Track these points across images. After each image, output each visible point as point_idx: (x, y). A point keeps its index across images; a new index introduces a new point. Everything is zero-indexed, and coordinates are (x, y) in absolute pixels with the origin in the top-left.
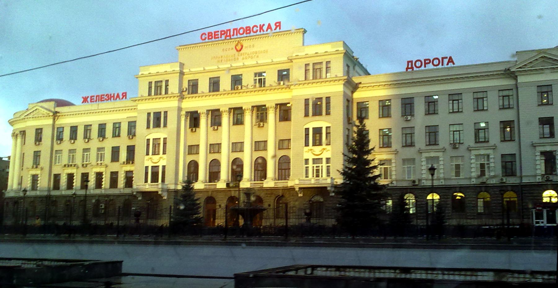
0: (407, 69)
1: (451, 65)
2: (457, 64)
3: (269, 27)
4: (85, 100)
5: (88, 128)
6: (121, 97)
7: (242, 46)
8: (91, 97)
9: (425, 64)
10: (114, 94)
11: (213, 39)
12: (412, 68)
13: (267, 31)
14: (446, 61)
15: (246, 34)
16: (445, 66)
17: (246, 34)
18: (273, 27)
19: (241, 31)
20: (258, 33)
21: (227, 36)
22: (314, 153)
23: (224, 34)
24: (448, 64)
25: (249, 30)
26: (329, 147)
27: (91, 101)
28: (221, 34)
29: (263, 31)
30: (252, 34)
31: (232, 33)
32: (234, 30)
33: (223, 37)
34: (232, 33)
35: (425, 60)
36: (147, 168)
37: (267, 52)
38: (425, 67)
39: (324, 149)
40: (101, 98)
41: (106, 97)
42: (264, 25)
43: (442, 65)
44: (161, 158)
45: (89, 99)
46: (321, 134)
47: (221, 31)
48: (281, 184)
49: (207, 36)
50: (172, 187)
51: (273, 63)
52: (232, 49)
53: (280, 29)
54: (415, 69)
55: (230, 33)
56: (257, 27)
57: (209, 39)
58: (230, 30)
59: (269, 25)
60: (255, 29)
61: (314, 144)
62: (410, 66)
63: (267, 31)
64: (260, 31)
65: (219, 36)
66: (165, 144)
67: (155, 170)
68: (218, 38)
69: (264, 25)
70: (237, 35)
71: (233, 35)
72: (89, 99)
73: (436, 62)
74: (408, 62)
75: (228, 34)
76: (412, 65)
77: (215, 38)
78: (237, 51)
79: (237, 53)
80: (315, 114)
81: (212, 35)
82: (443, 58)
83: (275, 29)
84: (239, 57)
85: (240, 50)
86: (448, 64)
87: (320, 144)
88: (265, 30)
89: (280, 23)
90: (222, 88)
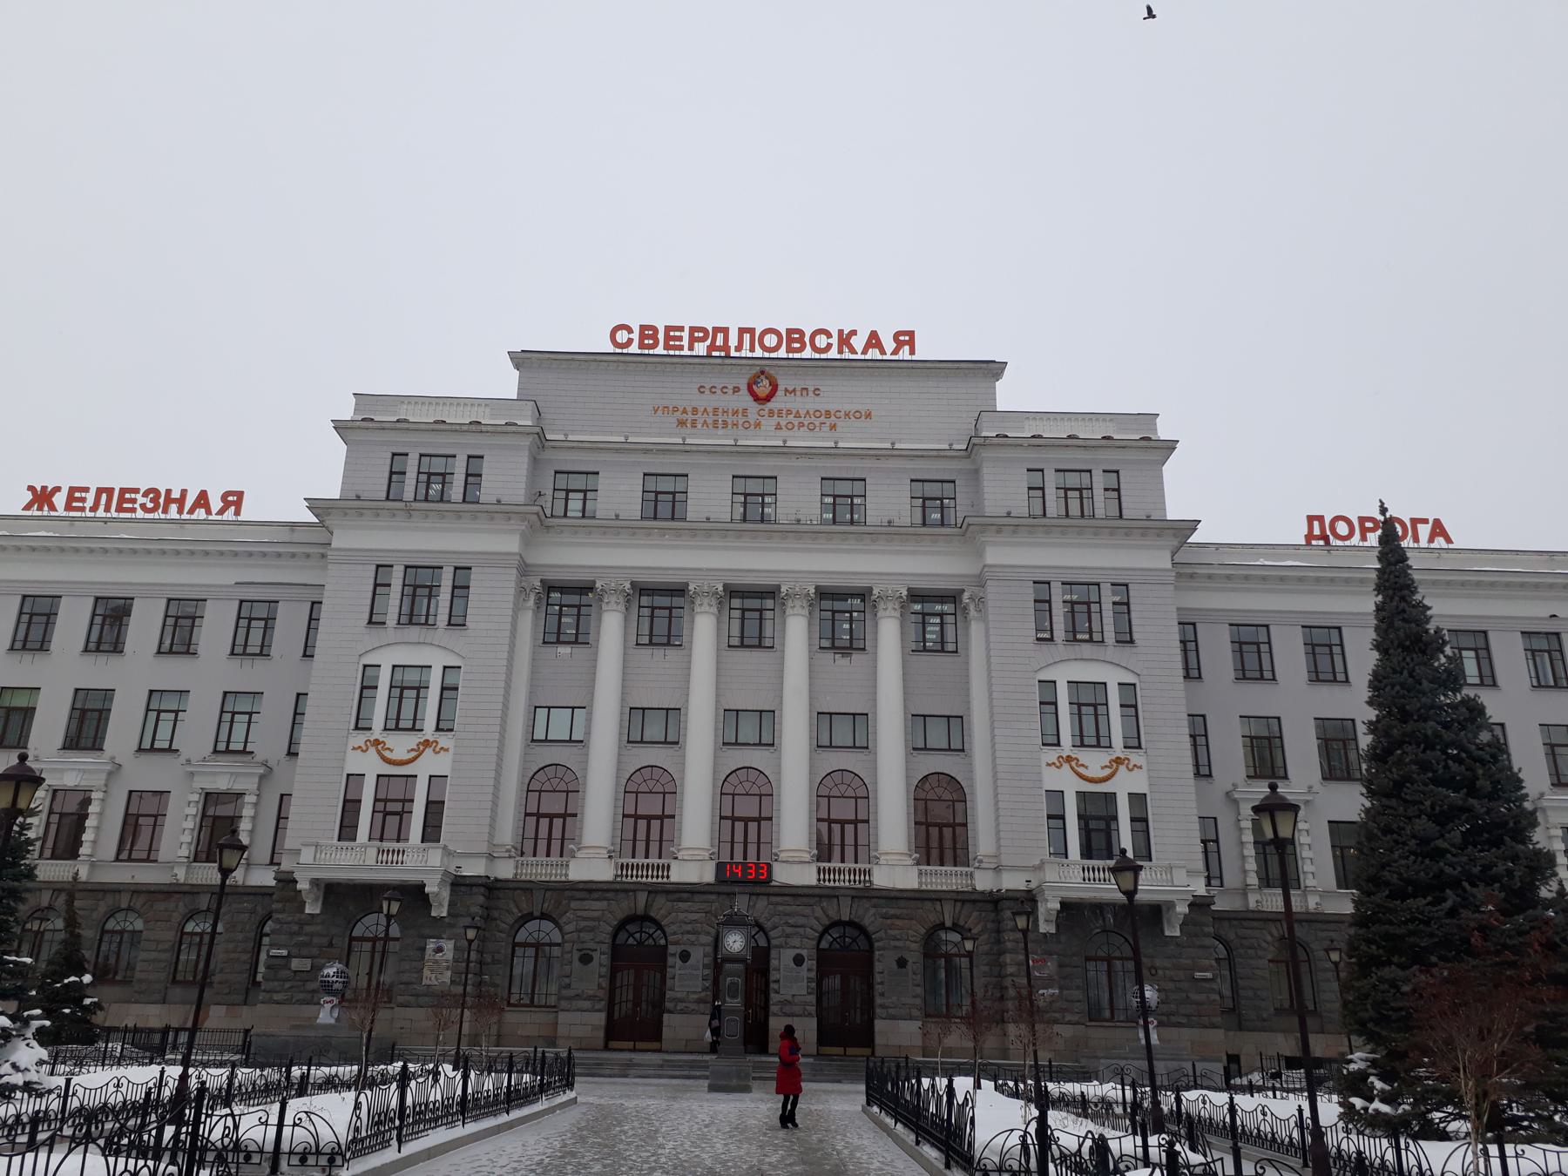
0: (1309, 537)
1: (1440, 542)
3: (874, 340)
7: (775, 388)
8: (72, 490)
10: (184, 492)
12: (1326, 539)
13: (865, 352)
16: (1423, 543)
18: (889, 345)
21: (712, 347)
22: (1081, 770)
24: (1431, 540)
25: (801, 340)
28: (693, 340)
29: (853, 351)
31: (733, 342)
32: (742, 331)
34: (733, 342)
35: (1362, 520)
36: (354, 779)
37: (868, 415)
39: (1118, 761)
40: (122, 500)
41: (141, 499)
42: (854, 333)
47: (693, 330)
48: (946, 879)
49: (635, 336)
50: (474, 868)
51: (892, 454)
52: (736, 390)
53: (912, 352)
54: (1334, 541)
55: (726, 339)
57: (642, 346)
58: (725, 331)
59: (874, 335)
60: (821, 341)
62: (1317, 532)
63: (865, 352)
64: (840, 351)
65: (685, 342)
66: (448, 689)
68: (681, 348)
69: (854, 333)
70: (752, 349)
71: (739, 348)
72: (60, 500)
74: (1311, 519)
75: (720, 341)
77: (667, 347)
78: (757, 398)
79: (753, 407)
80: (1073, 637)
81: (655, 337)
82: (1415, 522)
83: (895, 352)
85: (768, 398)
86: (1431, 540)
87: (1100, 742)
88: (859, 348)
89: (911, 334)
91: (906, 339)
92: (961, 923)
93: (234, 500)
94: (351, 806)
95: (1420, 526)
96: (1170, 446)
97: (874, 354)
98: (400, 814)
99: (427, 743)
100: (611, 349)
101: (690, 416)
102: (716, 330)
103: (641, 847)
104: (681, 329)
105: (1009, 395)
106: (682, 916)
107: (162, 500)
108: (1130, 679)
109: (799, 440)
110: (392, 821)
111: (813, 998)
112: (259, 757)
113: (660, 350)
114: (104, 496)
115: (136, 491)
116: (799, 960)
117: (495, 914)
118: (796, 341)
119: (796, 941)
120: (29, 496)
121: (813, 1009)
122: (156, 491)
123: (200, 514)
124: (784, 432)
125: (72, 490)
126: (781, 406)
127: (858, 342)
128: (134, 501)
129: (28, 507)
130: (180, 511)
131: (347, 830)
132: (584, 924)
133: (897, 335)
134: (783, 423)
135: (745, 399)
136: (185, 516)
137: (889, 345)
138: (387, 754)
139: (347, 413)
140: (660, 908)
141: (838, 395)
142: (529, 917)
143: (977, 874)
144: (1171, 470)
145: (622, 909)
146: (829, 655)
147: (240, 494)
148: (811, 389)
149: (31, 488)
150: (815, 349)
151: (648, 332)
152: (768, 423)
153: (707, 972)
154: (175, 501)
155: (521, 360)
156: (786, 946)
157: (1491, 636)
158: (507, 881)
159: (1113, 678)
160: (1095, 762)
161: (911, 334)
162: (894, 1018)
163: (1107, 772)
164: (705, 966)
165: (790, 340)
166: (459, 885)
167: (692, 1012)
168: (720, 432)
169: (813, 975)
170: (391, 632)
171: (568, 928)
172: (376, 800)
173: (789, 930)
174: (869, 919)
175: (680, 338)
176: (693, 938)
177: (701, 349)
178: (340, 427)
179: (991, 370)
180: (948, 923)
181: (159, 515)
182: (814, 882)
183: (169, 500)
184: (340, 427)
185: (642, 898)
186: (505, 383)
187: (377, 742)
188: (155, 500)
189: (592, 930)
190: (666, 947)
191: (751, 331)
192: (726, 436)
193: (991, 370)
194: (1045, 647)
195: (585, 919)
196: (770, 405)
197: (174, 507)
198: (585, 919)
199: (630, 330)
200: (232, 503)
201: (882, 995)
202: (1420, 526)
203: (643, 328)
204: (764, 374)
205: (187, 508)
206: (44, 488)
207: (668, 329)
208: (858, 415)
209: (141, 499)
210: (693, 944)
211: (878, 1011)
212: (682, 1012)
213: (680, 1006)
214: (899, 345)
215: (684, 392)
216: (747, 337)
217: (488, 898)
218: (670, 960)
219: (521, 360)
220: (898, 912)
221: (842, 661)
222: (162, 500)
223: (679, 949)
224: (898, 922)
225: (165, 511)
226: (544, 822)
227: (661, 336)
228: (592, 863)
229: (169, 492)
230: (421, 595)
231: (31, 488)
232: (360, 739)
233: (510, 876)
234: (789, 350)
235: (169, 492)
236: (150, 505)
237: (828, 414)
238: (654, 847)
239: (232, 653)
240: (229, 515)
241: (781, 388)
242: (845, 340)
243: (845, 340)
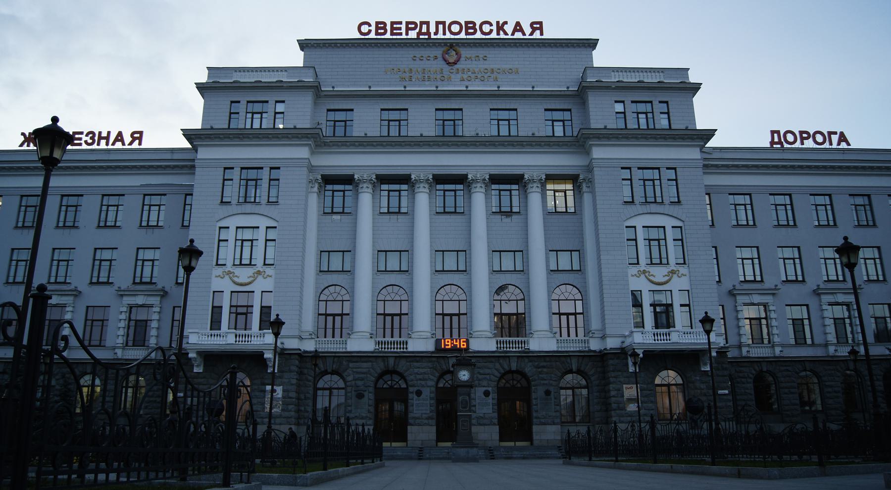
0: (772, 143)
1: (844, 145)
2: (856, 143)
3: (518, 27)
9: (802, 139)
10: (109, 133)
12: (780, 143)
13: (513, 34)
14: (835, 138)
22: (651, 278)
24: (839, 144)
25: (474, 28)
26: (683, 270)
28: (408, 29)
29: (506, 34)
31: (433, 29)
32: (438, 23)
34: (433, 29)
35: (801, 133)
38: (802, 144)
41: (84, 138)
42: (506, 23)
47: (408, 23)
49: (373, 28)
52: (436, 58)
53: (542, 34)
56: (491, 25)
57: (377, 34)
58: (427, 23)
59: (518, 24)
60: (486, 28)
62: (776, 140)
63: (513, 34)
64: (498, 34)
65: (403, 31)
68: (401, 34)
69: (506, 23)
70: (444, 34)
71: (436, 33)
74: (773, 132)
75: (424, 30)
77: (392, 34)
78: (448, 63)
79: (447, 68)
81: (384, 28)
82: (830, 133)
83: (531, 34)
84: (453, 76)
85: (455, 63)
86: (839, 144)
88: (509, 31)
89: (541, 23)
91: (537, 26)
92: (582, 369)
93: (138, 136)
94: (216, 311)
96: (696, 88)
97: (518, 35)
98: (246, 314)
99: (259, 273)
100: (359, 36)
101: (408, 75)
102: (422, 23)
103: (388, 332)
104: (400, 23)
105: (601, 58)
106: (416, 370)
107: (96, 138)
108: (679, 224)
109: (475, 87)
110: (241, 318)
111: (496, 415)
112: (160, 286)
113: (388, 36)
115: (82, 133)
116: (487, 394)
117: (305, 371)
119: (485, 383)
120: (22, 138)
121: (496, 421)
122: (93, 133)
123: (119, 145)
124: (467, 83)
126: (463, 66)
127: (509, 28)
128: (80, 139)
129: (21, 145)
130: (107, 144)
131: (215, 323)
132: (357, 376)
133: (532, 24)
134: (465, 76)
135: (441, 63)
136: (110, 147)
137: (528, 30)
138: (236, 279)
139: (204, 78)
140: (402, 366)
141: (497, 59)
142: (326, 373)
143: (591, 340)
144: (698, 100)
145: (380, 366)
146: (498, 217)
147: (141, 133)
148: (481, 56)
150: (483, 33)
151: (380, 26)
152: (456, 78)
153: (432, 402)
154: (104, 138)
155: (304, 45)
156: (480, 386)
157: (873, 197)
158: (310, 352)
160: (659, 273)
161: (541, 23)
162: (544, 424)
163: (667, 278)
164: (431, 399)
165: (467, 28)
166: (283, 354)
167: (425, 424)
168: (427, 83)
169: (495, 402)
170: (234, 209)
171: (350, 378)
172: (231, 306)
173: (480, 377)
174: (528, 369)
175: (400, 29)
176: (423, 383)
177: (413, 34)
178: (201, 87)
179: (592, 44)
180: (574, 368)
181: (95, 146)
182: (494, 349)
184: (201, 87)
185: (391, 361)
186: (297, 59)
187: (229, 273)
188: (93, 138)
189: (362, 379)
190: (407, 388)
191: (444, 23)
192: (431, 86)
193: (592, 44)
194: (629, 207)
195: (357, 373)
196: (456, 66)
197: (103, 142)
198: (357, 373)
199: (370, 25)
201: (537, 411)
203: (377, 23)
204: (452, 47)
205: (111, 141)
207: (392, 23)
209: (84, 138)
210: (423, 386)
211: (535, 420)
212: (419, 425)
213: (418, 421)
214: (534, 30)
215: (404, 59)
216: (441, 27)
217: (300, 362)
218: (410, 396)
219: (304, 45)
220: (545, 364)
221: (506, 220)
222: (96, 138)
223: (416, 389)
224: (545, 370)
225: (98, 144)
226: (330, 319)
227: (388, 28)
228: (361, 341)
229: (100, 133)
230: (252, 184)
231: (23, 134)
232: (219, 271)
233: (312, 349)
234: (467, 33)
235: (100, 133)
236: (90, 141)
237: (492, 71)
238: (396, 332)
239: (141, 226)
240: (136, 145)
241: (463, 56)
242: (500, 27)
243: (500, 27)
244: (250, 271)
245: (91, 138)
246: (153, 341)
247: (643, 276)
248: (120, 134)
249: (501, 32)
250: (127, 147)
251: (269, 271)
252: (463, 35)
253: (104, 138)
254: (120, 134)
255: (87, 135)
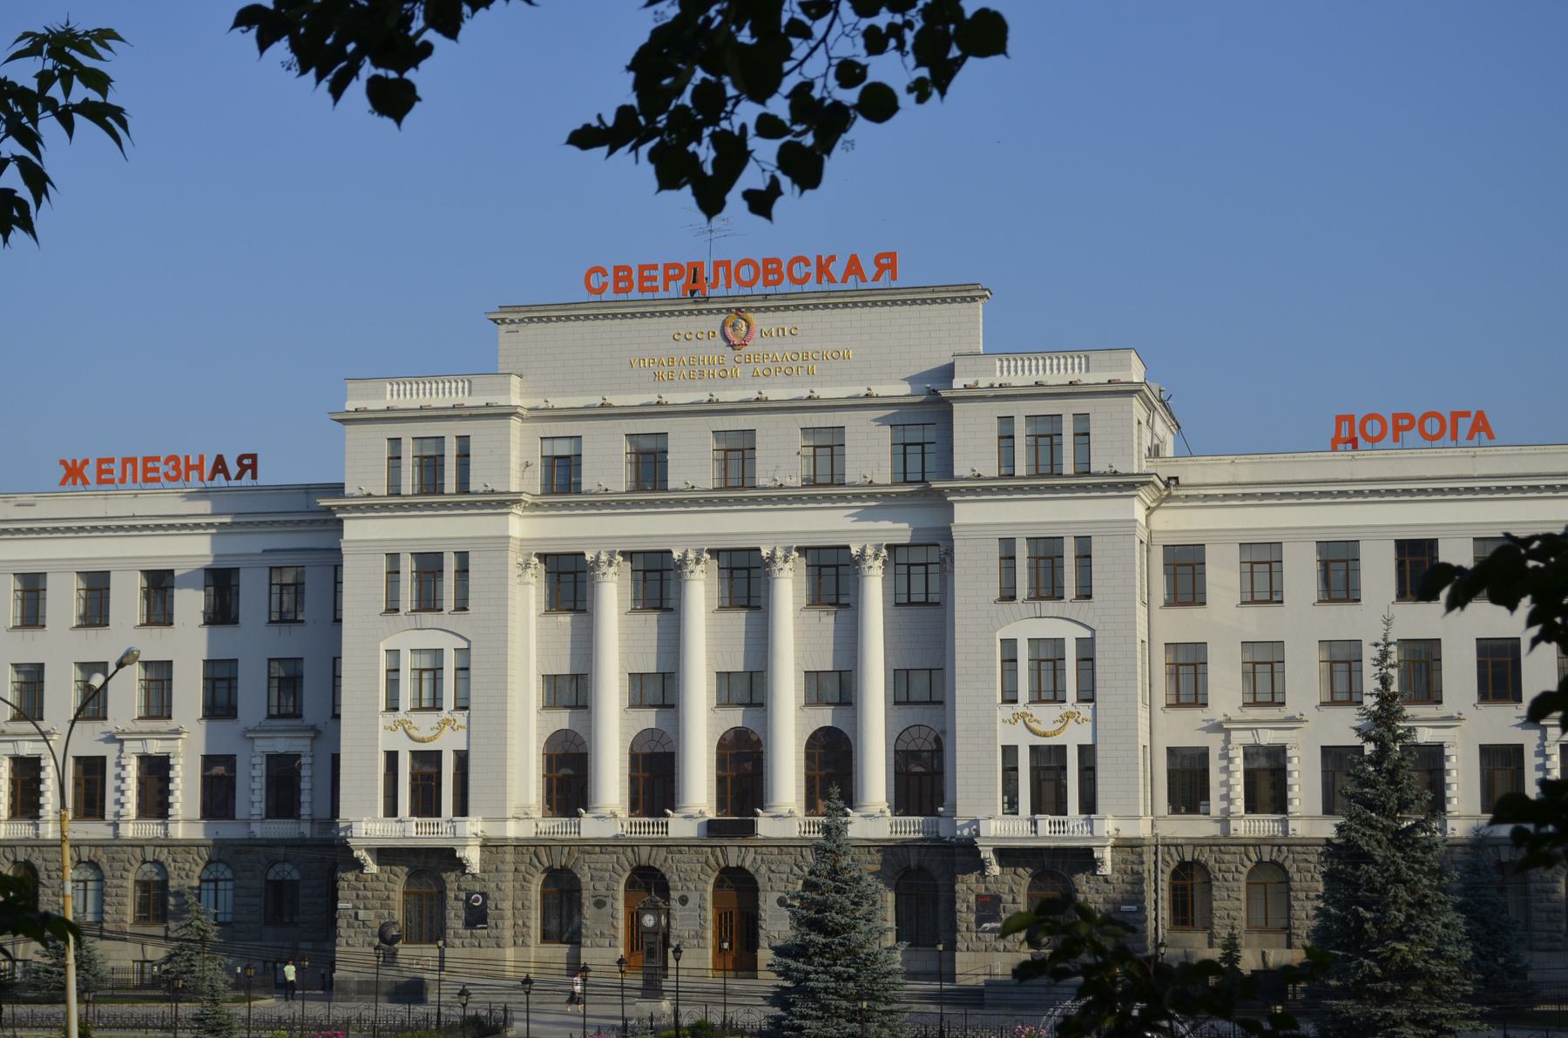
3: (854, 266)
4: (74, 472)
5: (97, 587)
6: (234, 469)
8: (100, 461)
9: (1398, 429)
10: (201, 458)
11: (635, 294)
13: (844, 280)
14: (1465, 425)
15: (767, 283)
17: (767, 283)
18: (870, 269)
19: (746, 273)
20: (811, 285)
23: (676, 278)
25: (778, 271)
27: (100, 481)
28: (667, 279)
29: (832, 280)
30: (786, 286)
32: (717, 264)
33: (676, 288)
35: (1396, 417)
38: (1396, 439)
40: (146, 470)
42: (832, 258)
43: (1454, 436)
44: (446, 722)
45: (90, 472)
46: (1057, 662)
47: (667, 267)
49: (610, 279)
54: (1361, 441)
56: (807, 264)
57: (617, 290)
59: (854, 260)
61: (1038, 699)
62: (1345, 434)
63: (844, 280)
64: (819, 281)
65: (660, 283)
66: (463, 670)
67: (427, 761)
68: (655, 289)
69: (832, 258)
70: (728, 285)
71: (715, 285)
72: (90, 472)
73: (1432, 426)
74: (1340, 419)
76: (1352, 430)
77: (642, 289)
80: (1036, 596)
81: (628, 278)
82: (1456, 416)
87: (1057, 698)
88: (838, 276)
89: (892, 256)
90: (676, 477)
91: (887, 263)
93: (249, 463)
95: (1461, 420)
100: (583, 295)
104: (655, 267)
107: (182, 467)
109: (775, 393)
114: (129, 467)
115: (158, 459)
118: (773, 272)
120: (62, 471)
122: (174, 458)
124: (762, 380)
125: (100, 461)
127: (837, 269)
130: (201, 479)
137: (870, 269)
140: (658, 860)
149: (63, 462)
150: (793, 280)
154: (194, 467)
159: (1070, 634)
163: (1059, 725)
165: (767, 272)
168: (699, 383)
175: (654, 279)
183: (189, 468)
191: (727, 264)
197: (194, 475)
199: (605, 274)
200: (248, 467)
202: (1461, 420)
203: (617, 269)
206: (74, 461)
208: (837, 355)
214: (881, 269)
222: (182, 467)
227: (635, 276)
231: (63, 462)
235: (187, 458)
236: (173, 473)
240: (247, 480)
243: (823, 269)
244: (432, 718)
245: (174, 468)
246: (305, 810)
247: (1020, 721)
248: (220, 460)
249: (825, 278)
250: (233, 483)
251: (461, 717)
252: (759, 288)
253: (194, 467)
254: (220, 460)
255: (166, 463)
